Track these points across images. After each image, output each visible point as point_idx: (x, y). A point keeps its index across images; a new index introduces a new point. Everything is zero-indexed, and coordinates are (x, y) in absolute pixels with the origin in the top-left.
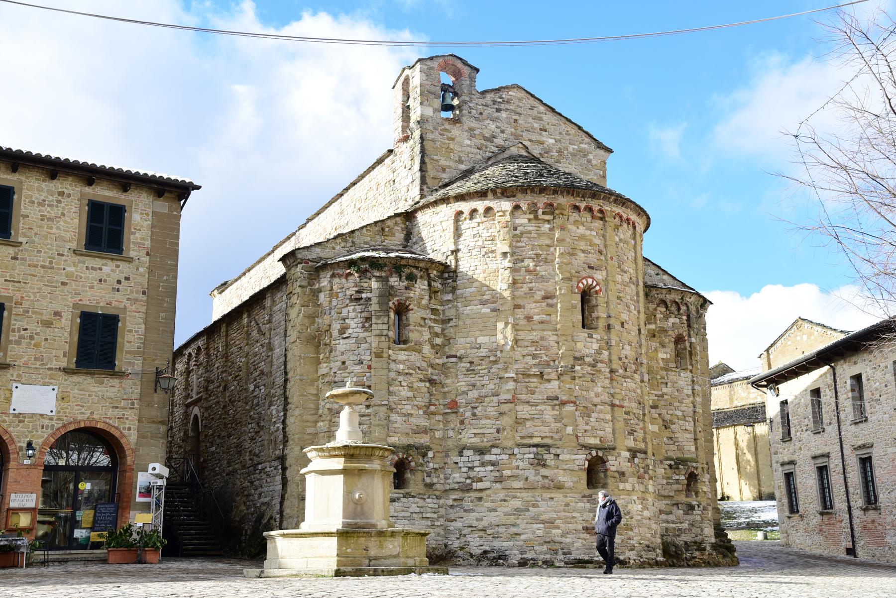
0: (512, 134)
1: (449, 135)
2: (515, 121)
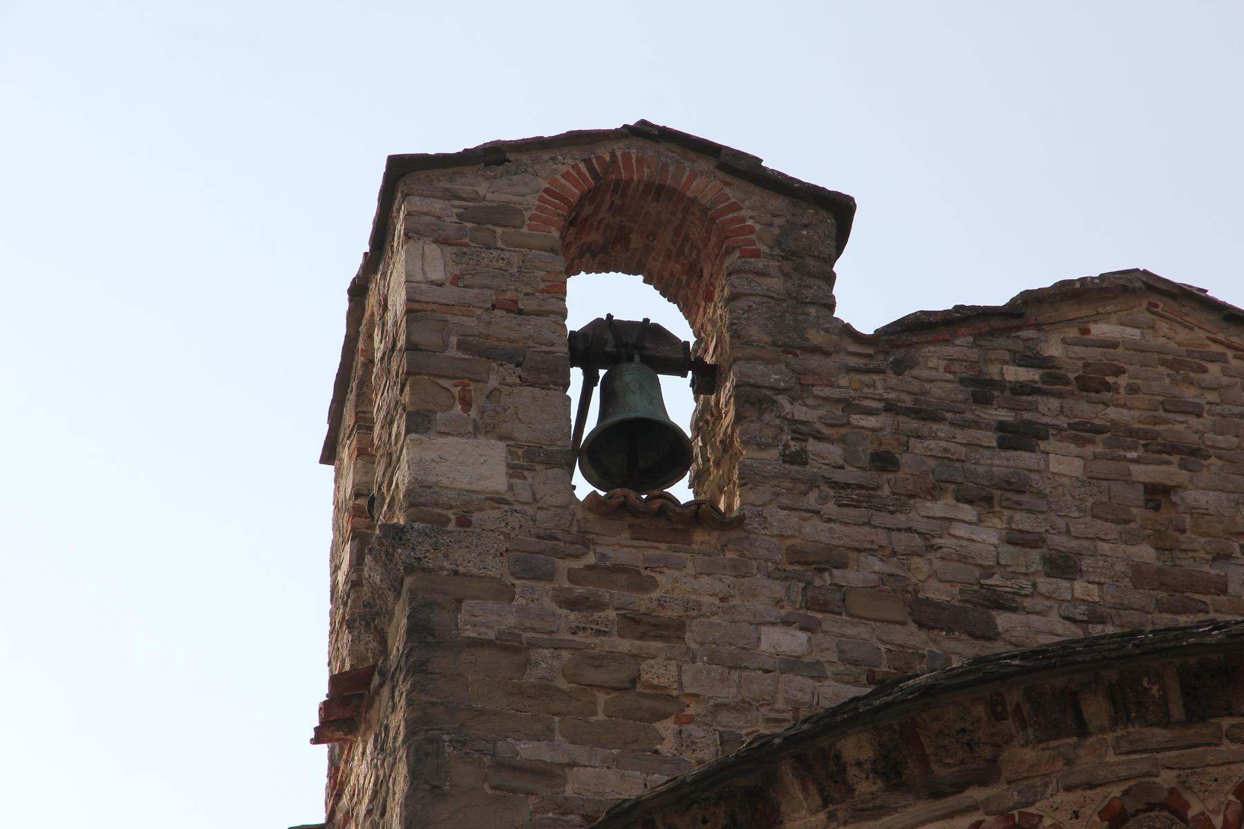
0: (1140, 576)
1: (643, 602)
2: (1157, 494)
